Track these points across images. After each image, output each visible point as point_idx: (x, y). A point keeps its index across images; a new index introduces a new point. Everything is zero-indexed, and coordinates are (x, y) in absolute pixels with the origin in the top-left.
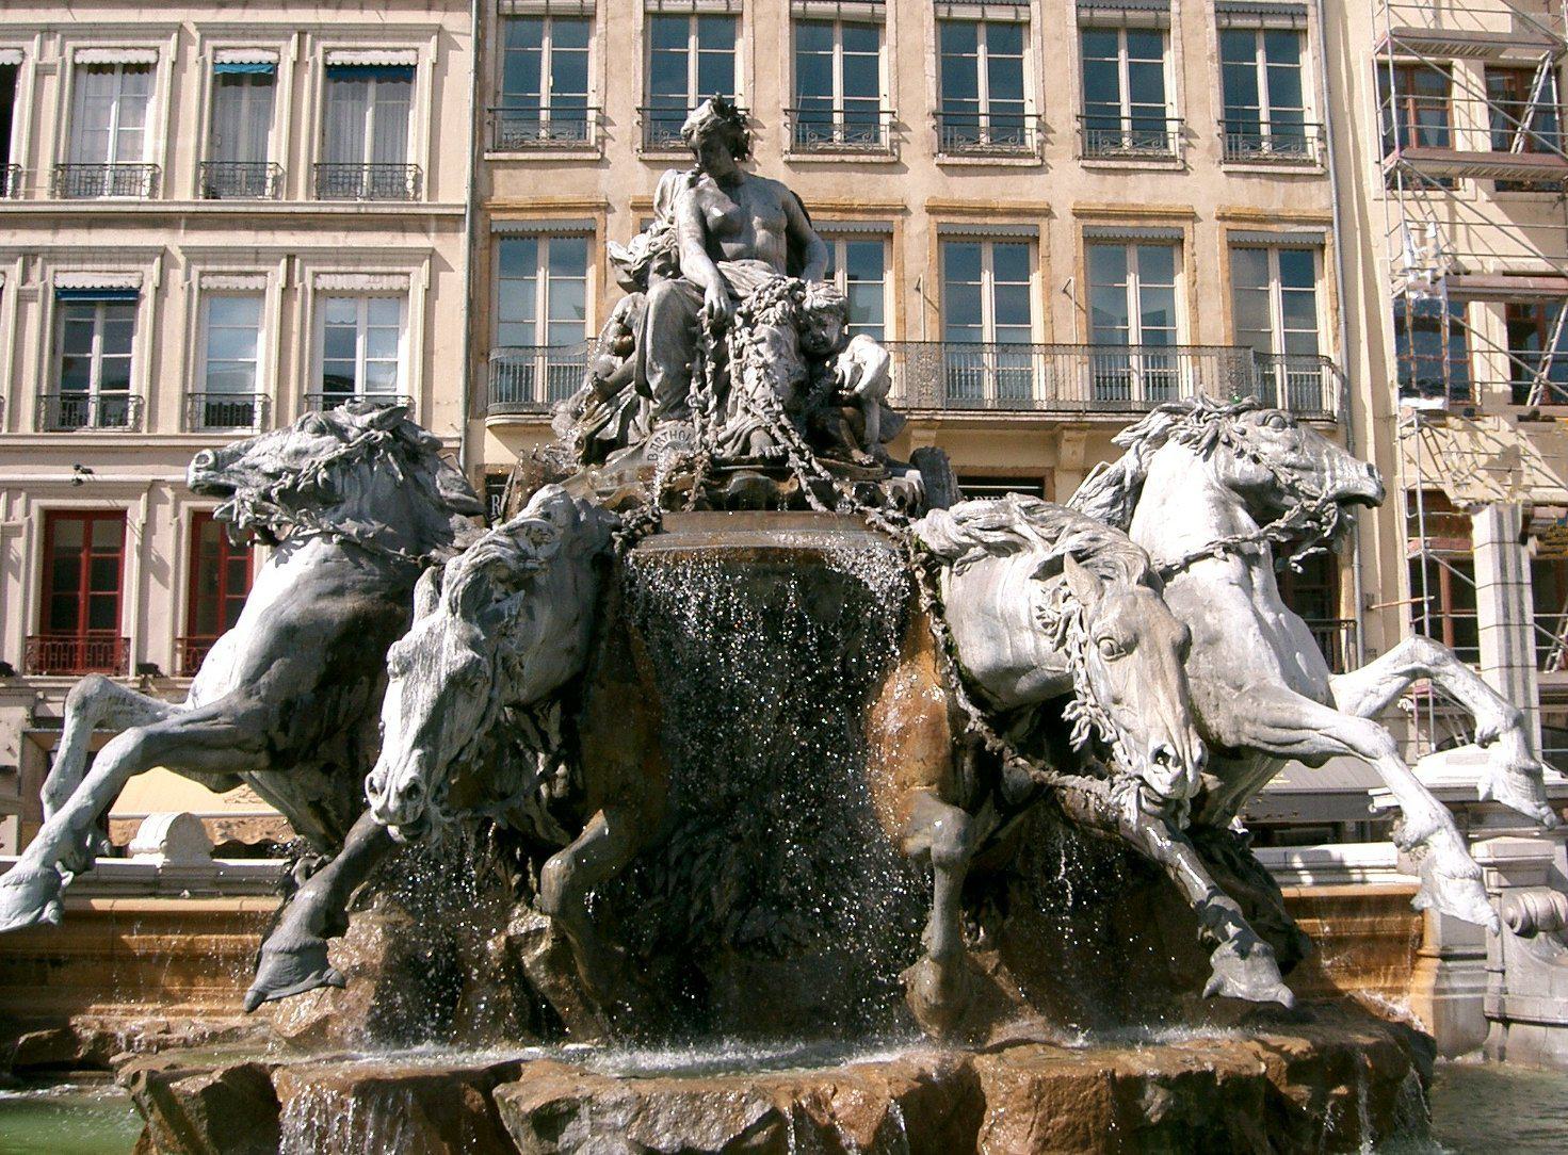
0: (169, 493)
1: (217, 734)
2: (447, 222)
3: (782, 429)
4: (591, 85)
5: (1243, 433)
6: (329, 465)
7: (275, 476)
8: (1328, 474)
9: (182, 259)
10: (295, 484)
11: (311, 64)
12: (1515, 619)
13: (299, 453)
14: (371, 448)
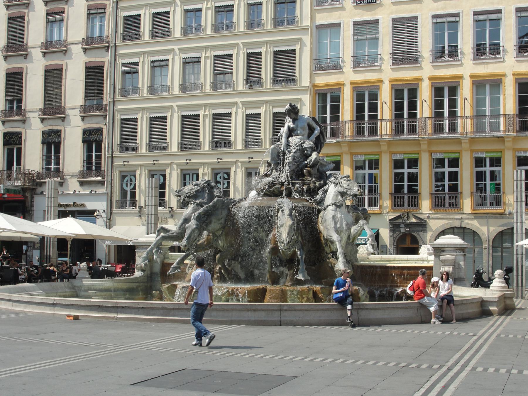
0: (240, 164)
1: (173, 236)
2: (304, 90)
3: (287, 176)
4: (340, 51)
5: (342, 182)
6: (196, 191)
7: (187, 193)
9: (240, 105)
10: (190, 195)
11: (270, 51)
12: (519, 200)
13: (191, 189)
14: (203, 187)
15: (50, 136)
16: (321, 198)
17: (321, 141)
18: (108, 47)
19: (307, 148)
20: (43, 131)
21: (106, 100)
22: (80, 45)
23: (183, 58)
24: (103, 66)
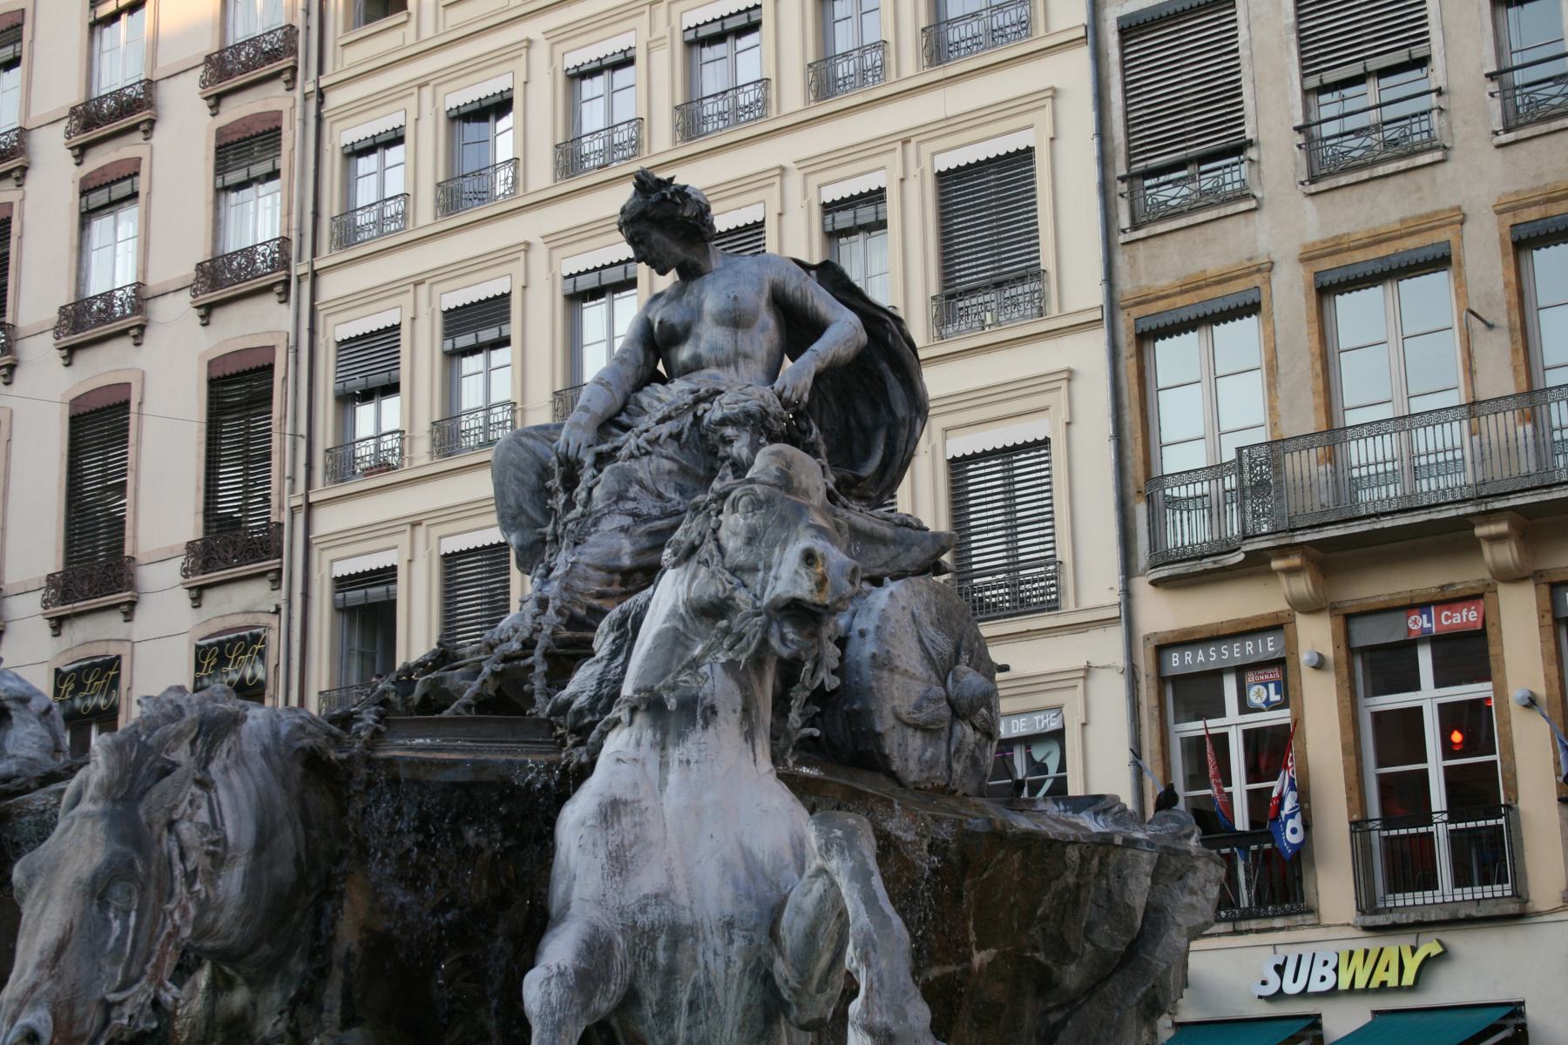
8: (772, 573)
15: (80, 687)
16: (600, 684)
17: (891, 412)
18: (287, 283)
19: (724, 422)
20: (57, 671)
21: (281, 507)
22: (187, 293)
23: (566, 278)
24: (270, 368)
